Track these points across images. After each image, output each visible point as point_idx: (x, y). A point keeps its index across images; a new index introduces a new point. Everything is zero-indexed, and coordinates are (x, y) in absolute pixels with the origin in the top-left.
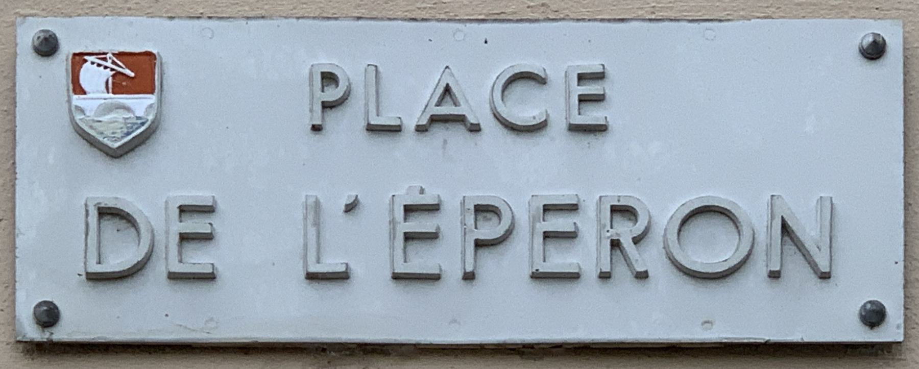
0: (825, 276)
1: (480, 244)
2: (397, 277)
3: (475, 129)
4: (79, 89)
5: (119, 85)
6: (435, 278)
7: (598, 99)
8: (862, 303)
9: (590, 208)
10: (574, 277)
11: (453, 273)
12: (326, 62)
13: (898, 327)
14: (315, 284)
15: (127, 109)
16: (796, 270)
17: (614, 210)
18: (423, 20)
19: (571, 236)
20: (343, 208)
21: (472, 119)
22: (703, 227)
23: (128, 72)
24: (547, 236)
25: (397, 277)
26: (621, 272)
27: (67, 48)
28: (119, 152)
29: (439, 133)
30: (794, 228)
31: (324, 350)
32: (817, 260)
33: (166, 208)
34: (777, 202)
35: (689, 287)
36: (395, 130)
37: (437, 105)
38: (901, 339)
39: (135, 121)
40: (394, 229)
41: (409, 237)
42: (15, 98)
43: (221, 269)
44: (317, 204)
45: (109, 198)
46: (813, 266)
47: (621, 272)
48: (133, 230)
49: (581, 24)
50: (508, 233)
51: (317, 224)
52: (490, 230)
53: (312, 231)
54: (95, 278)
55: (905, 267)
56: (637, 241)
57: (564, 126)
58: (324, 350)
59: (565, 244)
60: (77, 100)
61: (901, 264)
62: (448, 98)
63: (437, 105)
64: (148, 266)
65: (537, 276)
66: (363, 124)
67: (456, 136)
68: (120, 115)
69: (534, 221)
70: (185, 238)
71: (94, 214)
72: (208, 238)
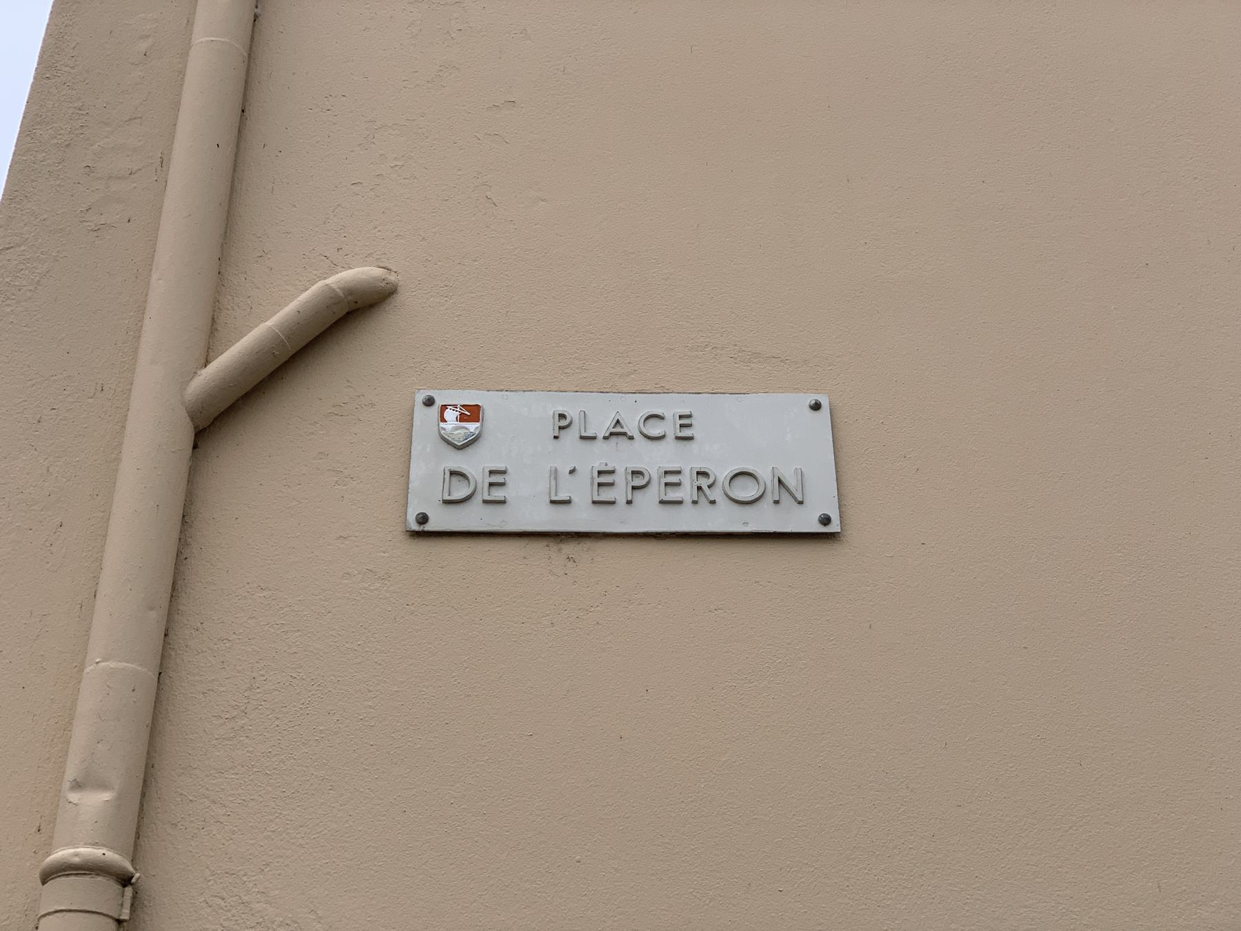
0: (801, 503)
1: (634, 488)
2: (594, 502)
3: (631, 438)
4: (443, 420)
5: (462, 418)
6: (613, 503)
7: (689, 426)
8: (820, 514)
9: (687, 472)
10: (680, 503)
11: (622, 501)
12: (561, 410)
13: (838, 526)
14: (584, 441)
15: (466, 429)
16: (786, 499)
17: (698, 473)
18: (607, 392)
19: (678, 484)
20: (568, 472)
21: (630, 434)
22: (741, 481)
23: (467, 413)
24: (666, 484)
25: (594, 502)
26: (703, 500)
27: (439, 402)
28: (462, 447)
29: (614, 440)
30: (785, 482)
31: (559, 535)
32: (796, 496)
33: (483, 471)
34: (776, 472)
35: (735, 507)
36: (594, 438)
37: (613, 428)
38: (839, 531)
39: (469, 433)
40: (593, 482)
41: (600, 485)
42: (412, 424)
43: (508, 499)
44: (556, 469)
45: (455, 466)
46: (795, 498)
47: (703, 500)
48: (466, 481)
49: (679, 395)
50: (648, 483)
51: (556, 478)
52: (639, 482)
53: (553, 483)
54: (447, 502)
55: (839, 499)
56: (709, 487)
57: (673, 437)
58: (559, 535)
59: (676, 488)
60: (442, 425)
61: (837, 497)
62: (618, 424)
63: (613, 428)
64: (472, 498)
65: (662, 502)
66: (578, 436)
67: (622, 441)
68: (462, 432)
69: (660, 478)
70: (491, 485)
71: (448, 474)
72: (502, 484)
